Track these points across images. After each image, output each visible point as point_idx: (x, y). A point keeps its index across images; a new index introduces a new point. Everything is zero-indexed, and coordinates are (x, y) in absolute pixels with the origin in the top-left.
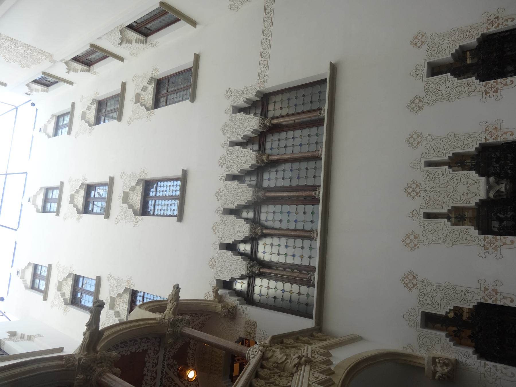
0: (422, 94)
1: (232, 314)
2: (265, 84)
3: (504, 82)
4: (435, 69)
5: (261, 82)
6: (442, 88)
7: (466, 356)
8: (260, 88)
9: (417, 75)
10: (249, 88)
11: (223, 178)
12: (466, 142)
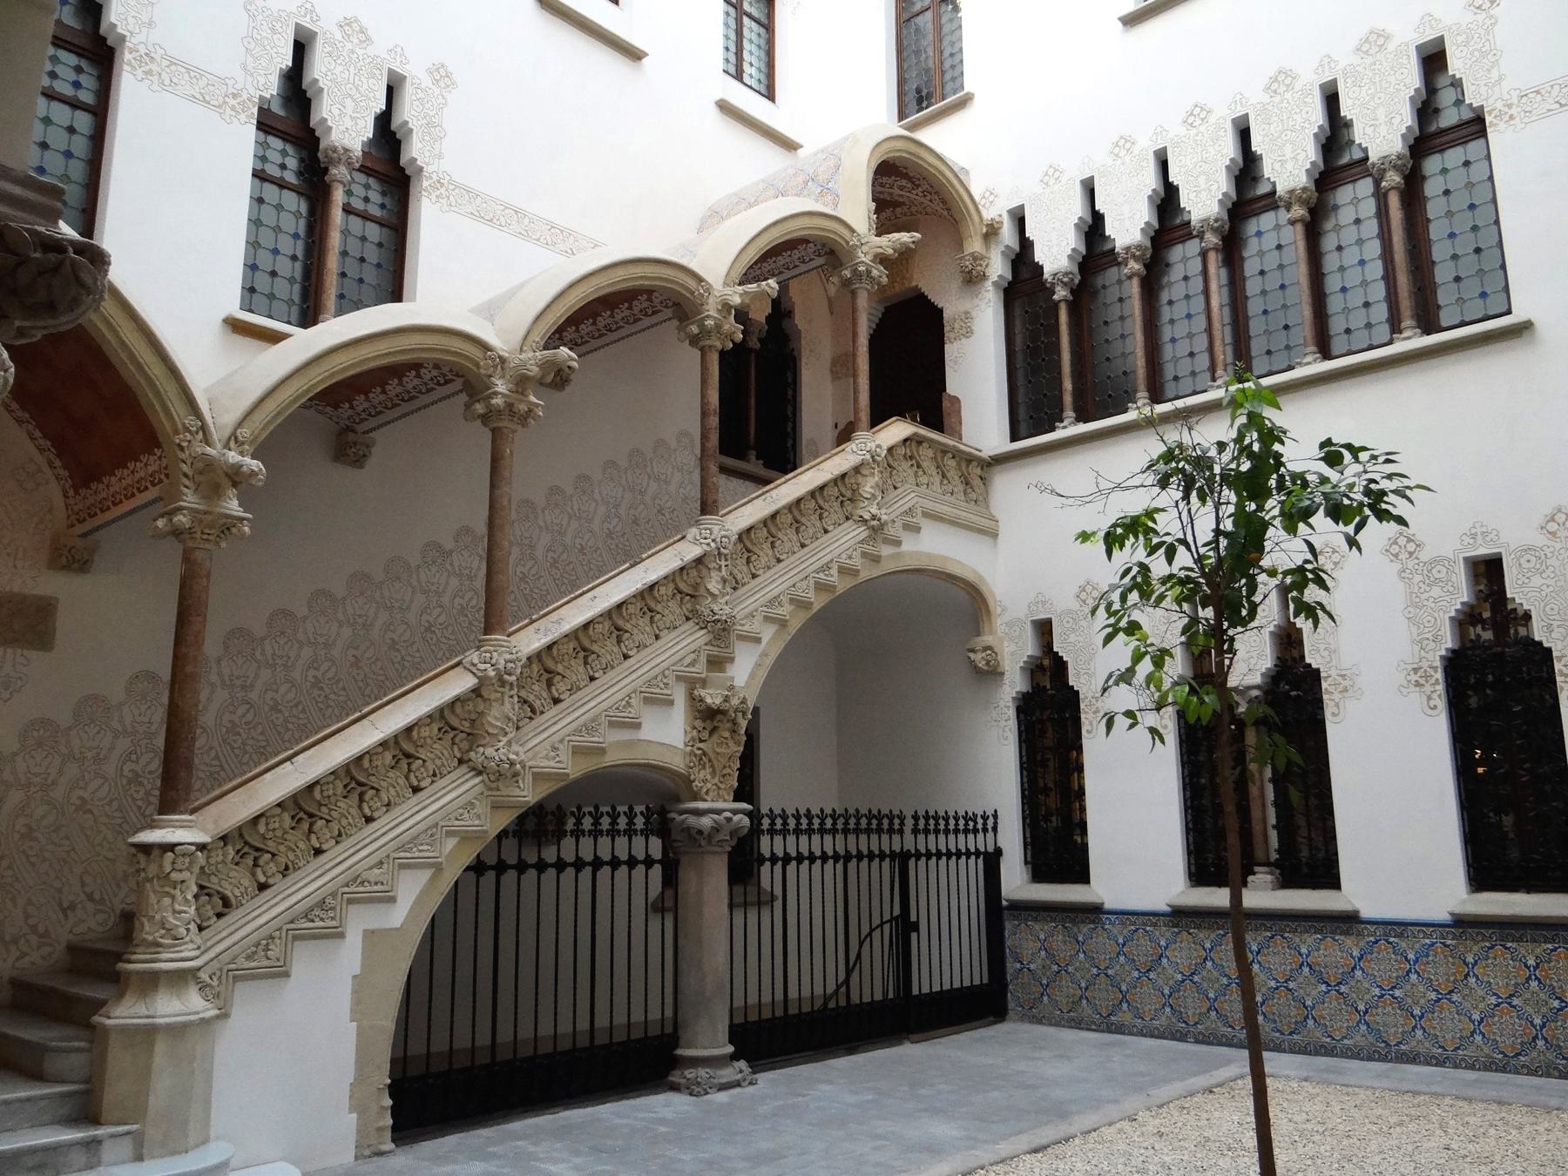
0: (1425, 556)
1: (972, 279)
2: (1502, 126)
3: (1435, 696)
4: (1488, 571)
5: (1510, 106)
6: (1436, 592)
7: (1014, 683)
8: (1490, 112)
9: (1474, 536)
10: (1495, 74)
11: (1239, 108)
12: (1322, 647)
